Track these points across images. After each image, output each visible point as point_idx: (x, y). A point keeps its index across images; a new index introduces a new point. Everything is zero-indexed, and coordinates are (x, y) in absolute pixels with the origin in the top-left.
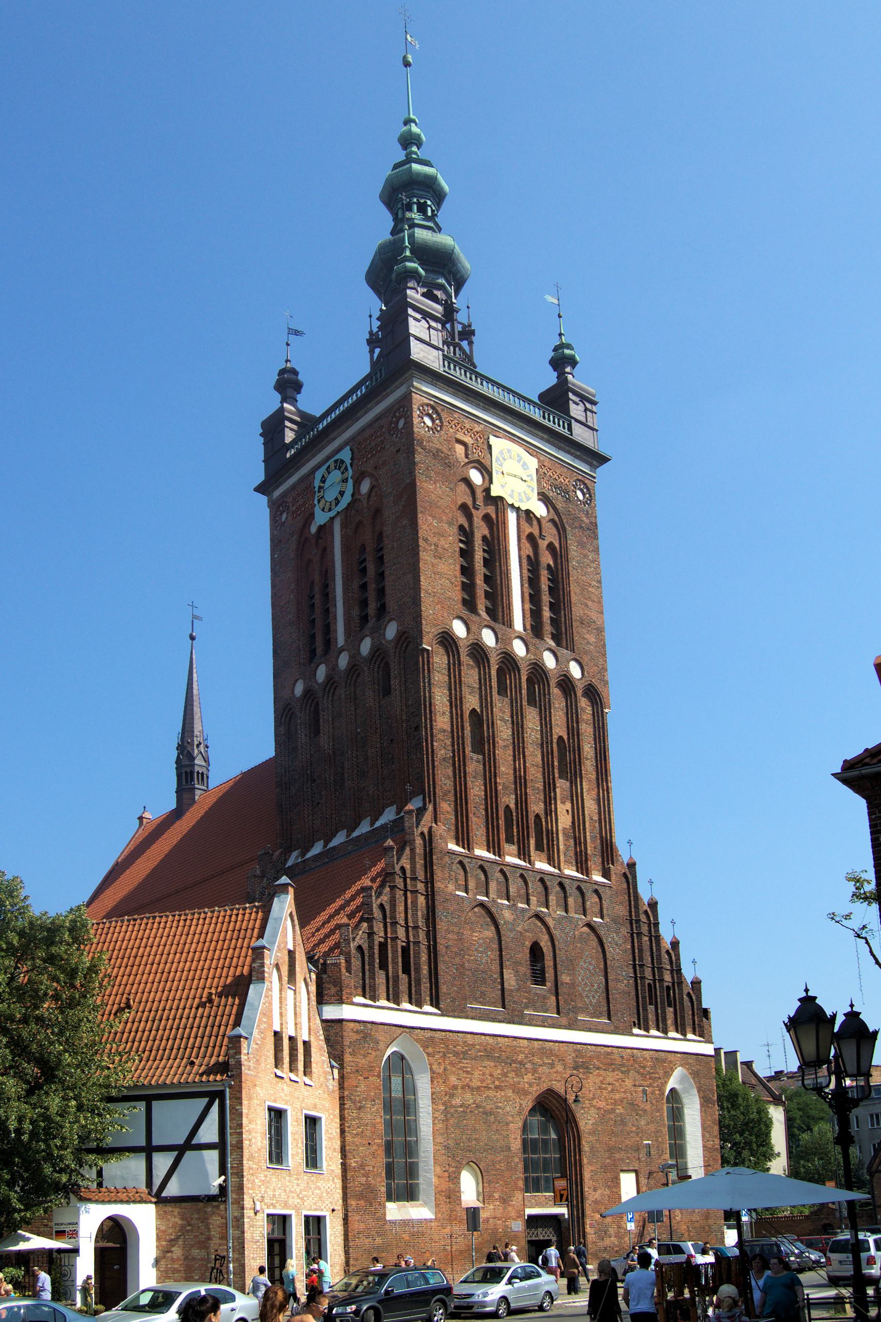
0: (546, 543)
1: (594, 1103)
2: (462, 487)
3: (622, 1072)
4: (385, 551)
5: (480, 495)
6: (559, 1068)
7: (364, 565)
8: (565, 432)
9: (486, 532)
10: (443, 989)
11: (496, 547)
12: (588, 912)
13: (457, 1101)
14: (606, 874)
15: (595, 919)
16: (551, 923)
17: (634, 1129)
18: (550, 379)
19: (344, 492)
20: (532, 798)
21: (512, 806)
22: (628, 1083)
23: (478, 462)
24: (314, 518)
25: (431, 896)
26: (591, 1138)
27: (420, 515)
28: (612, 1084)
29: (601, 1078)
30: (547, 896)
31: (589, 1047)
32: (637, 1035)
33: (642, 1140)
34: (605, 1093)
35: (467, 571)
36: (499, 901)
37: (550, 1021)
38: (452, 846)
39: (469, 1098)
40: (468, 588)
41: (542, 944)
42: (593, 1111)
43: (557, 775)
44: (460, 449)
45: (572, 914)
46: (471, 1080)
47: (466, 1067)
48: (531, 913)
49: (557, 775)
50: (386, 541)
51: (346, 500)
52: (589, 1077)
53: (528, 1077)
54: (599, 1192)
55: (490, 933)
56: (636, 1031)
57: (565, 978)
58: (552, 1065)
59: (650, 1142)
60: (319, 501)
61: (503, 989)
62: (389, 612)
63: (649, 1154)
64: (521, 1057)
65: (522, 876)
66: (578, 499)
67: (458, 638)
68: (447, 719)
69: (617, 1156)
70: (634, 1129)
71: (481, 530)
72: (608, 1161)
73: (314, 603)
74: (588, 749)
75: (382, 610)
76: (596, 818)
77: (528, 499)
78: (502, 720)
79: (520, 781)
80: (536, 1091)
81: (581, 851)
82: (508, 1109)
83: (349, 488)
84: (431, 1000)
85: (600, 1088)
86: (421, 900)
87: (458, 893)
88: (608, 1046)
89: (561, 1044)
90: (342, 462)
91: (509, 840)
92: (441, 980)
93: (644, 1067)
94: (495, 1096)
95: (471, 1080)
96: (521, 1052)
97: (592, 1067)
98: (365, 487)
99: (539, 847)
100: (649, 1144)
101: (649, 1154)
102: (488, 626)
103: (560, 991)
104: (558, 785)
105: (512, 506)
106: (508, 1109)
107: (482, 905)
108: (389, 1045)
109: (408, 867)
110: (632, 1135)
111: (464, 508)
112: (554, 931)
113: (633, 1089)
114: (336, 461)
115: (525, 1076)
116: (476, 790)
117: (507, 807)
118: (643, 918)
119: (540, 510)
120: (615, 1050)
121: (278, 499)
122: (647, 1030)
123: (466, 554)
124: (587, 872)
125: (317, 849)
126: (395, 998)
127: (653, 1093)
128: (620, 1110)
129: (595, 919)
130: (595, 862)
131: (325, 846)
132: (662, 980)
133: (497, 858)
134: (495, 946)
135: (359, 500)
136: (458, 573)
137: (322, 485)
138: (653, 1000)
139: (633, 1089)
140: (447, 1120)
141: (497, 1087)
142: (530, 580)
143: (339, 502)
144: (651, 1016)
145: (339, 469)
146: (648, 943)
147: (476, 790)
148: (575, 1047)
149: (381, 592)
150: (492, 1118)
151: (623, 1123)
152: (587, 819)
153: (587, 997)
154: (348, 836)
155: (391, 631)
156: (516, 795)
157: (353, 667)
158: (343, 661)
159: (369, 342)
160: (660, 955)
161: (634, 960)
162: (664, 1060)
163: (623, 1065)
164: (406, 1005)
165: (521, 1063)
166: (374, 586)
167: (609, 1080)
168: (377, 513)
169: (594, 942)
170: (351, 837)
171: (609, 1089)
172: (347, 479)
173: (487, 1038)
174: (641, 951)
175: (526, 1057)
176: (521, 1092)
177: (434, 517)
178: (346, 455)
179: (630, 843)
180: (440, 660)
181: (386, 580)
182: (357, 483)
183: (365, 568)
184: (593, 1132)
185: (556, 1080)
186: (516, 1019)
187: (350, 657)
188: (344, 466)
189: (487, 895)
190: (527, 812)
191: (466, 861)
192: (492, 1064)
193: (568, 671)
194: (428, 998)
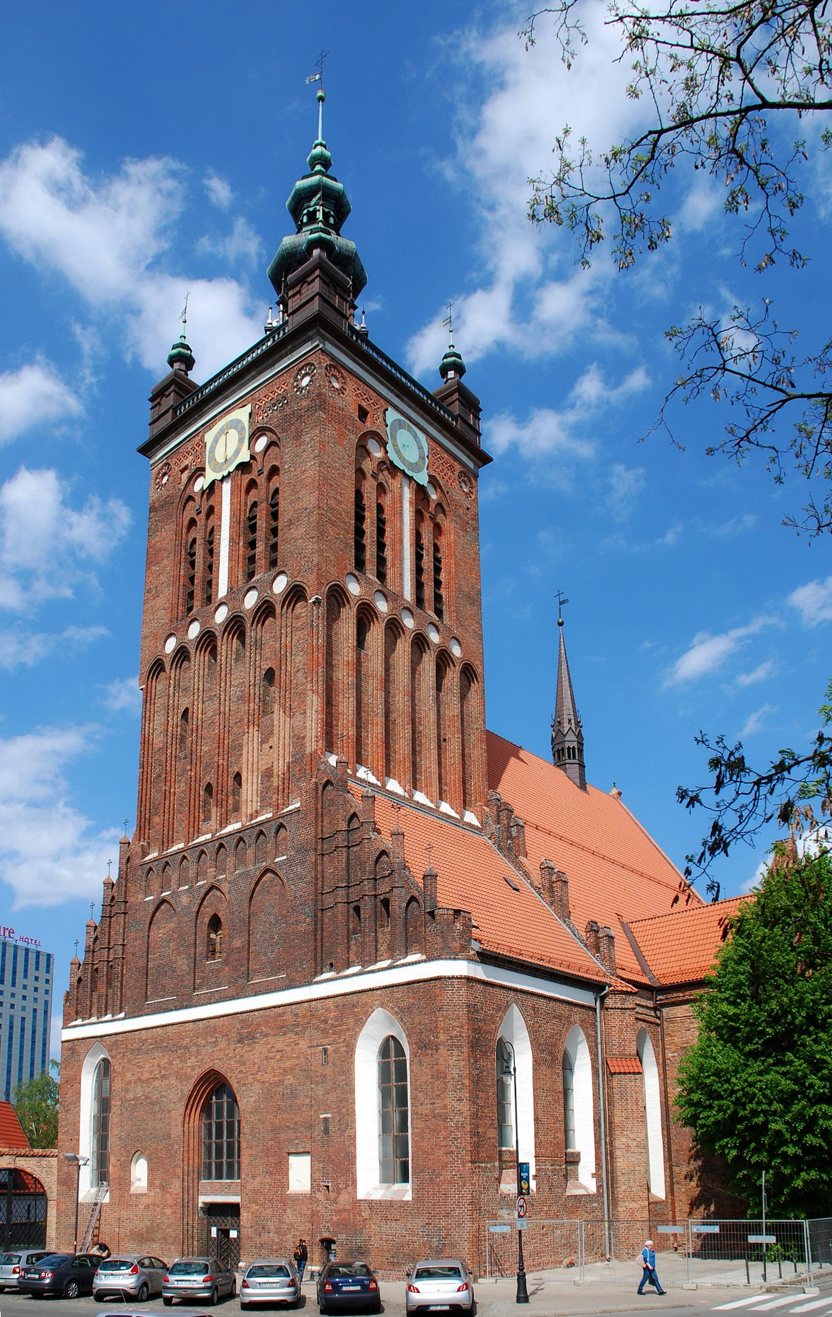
1: (258, 1077)
3: (297, 1033)
6: (223, 1044)
17: (308, 1101)
22: (303, 1045)
26: (252, 1118)
28: (282, 1051)
29: (269, 1046)
31: (256, 1013)
34: (273, 1063)
39: (139, 1091)
42: (257, 1087)
47: (139, 1062)
52: (255, 1048)
54: (258, 1179)
58: (215, 1043)
59: (329, 1115)
63: (326, 1131)
69: (283, 1136)
72: (271, 1143)
80: (197, 1073)
82: (171, 1096)
85: (267, 1058)
88: (279, 1006)
89: (226, 1018)
93: (325, 1021)
94: (160, 1085)
96: (187, 1036)
97: (259, 1035)
100: (326, 1119)
101: (326, 1131)
106: (171, 1096)
110: (304, 1109)
115: (188, 1061)
120: (289, 1008)
128: (289, 1080)
148: (240, 1017)
150: (157, 1108)
151: (293, 1095)
153: (265, 954)
163: (297, 1025)
165: (186, 1048)
167: (279, 1046)
171: (278, 1057)
173: (158, 1029)
175: (191, 1041)
176: (181, 1077)
184: (256, 1111)
185: (217, 1059)
186: (185, 1003)
192: (161, 1055)
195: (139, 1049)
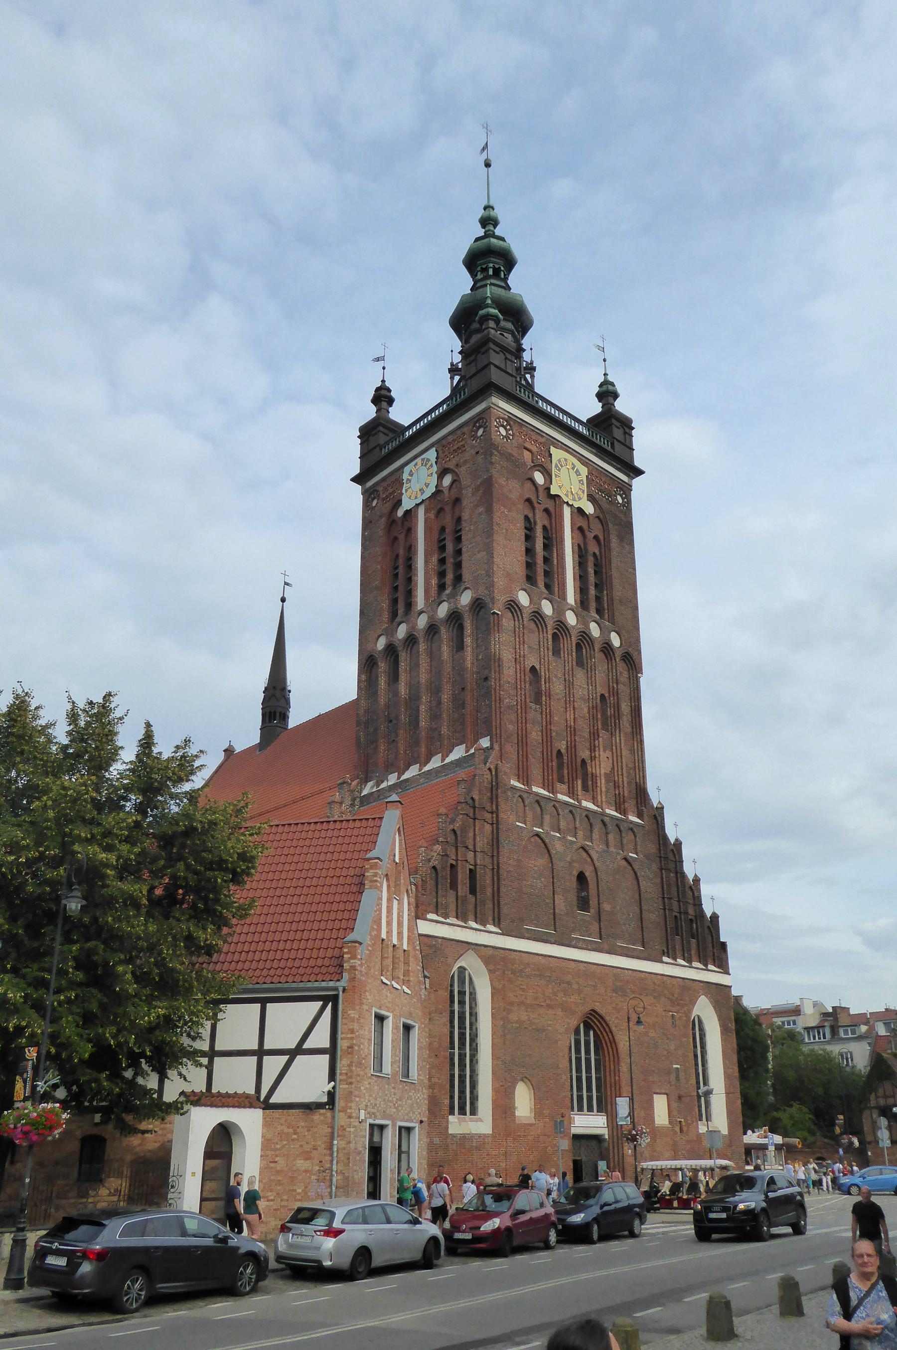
0: (593, 535)
2: (529, 485)
4: (463, 533)
5: (541, 490)
7: (443, 543)
8: (609, 449)
9: (546, 523)
10: (505, 910)
11: (554, 535)
12: (625, 848)
13: (513, 1017)
14: (640, 816)
15: (630, 854)
16: (595, 856)
18: (596, 408)
19: (429, 484)
20: (579, 746)
21: (563, 751)
23: (541, 466)
24: (401, 504)
25: (496, 824)
27: (494, 504)
30: (591, 831)
31: (626, 971)
32: (667, 963)
33: (672, 1064)
35: (529, 551)
36: (552, 833)
37: (594, 946)
38: (514, 783)
40: (530, 565)
41: (587, 874)
43: (600, 727)
44: (527, 455)
45: (612, 849)
46: (526, 998)
48: (579, 845)
49: (600, 727)
50: (464, 524)
51: (432, 489)
53: (575, 998)
55: (542, 861)
56: (665, 959)
57: (606, 907)
59: (679, 1066)
60: (406, 491)
61: (554, 915)
62: (465, 582)
63: (677, 1078)
64: (569, 977)
65: (571, 812)
66: (618, 503)
67: (522, 605)
68: (512, 671)
69: (651, 1078)
70: (665, 1053)
71: (541, 520)
73: (398, 573)
74: (625, 707)
75: (458, 579)
76: (631, 765)
77: (580, 499)
78: (556, 677)
79: (573, 731)
81: (619, 794)
83: (434, 481)
84: (494, 920)
86: (488, 828)
87: (517, 823)
90: (428, 460)
91: (561, 780)
92: (502, 903)
95: (526, 998)
98: (447, 480)
99: (585, 788)
100: (677, 1068)
101: (677, 1078)
102: (545, 598)
103: (602, 918)
104: (601, 735)
105: (567, 503)
107: (537, 835)
108: (457, 960)
109: (476, 797)
111: (529, 500)
112: (597, 864)
113: (664, 1014)
114: (423, 460)
116: (535, 736)
117: (559, 752)
118: (671, 857)
119: (589, 509)
121: (370, 488)
122: (675, 959)
123: (529, 537)
124: (624, 812)
125: (392, 779)
126: (462, 916)
127: (680, 1018)
129: (630, 854)
130: (630, 804)
131: (399, 778)
132: (686, 913)
133: (551, 795)
134: (548, 873)
135: (442, 491)
136: (524, 553)
137: (410, 478)
138: (677, 931)
139: (664, 1014)
140: (504, 1035)
141: (548, 1006)
142: (580, 564)
143: (424, 492)
144: (678, 947)
145: (425, 466)
146: (675, 879)
147: (535, 736)
148: (615, 970)
149: (458, 565)
152: (624, 766)
154: (420, 770)
155: (466, 599)
156: (567, 741)
157: (432, 629)
158: (422, 622)
159: (450, 371)
160: (685, 890)
161: (663, 894)
162: (690, 989)
164: (473, 924)
165: (569, 983)
166: (452, 560)
168: (457, 501)
169: (630, 875)
170: (423, 771)
172: (432, 474)
174: (669, 885)
177: (505, 507)
178: (432, 454)
179: (659, 789)
180: (507, 622)
181: (463, 556)
182: (441, 476)
183: (444, 545)
187: (429, 617)
188: (430, 463)
189: (541, 826)
190: (576, 756)
191: (525, 796)
193: (610, 640)
194: (490, 918)
195: (522, 971)
